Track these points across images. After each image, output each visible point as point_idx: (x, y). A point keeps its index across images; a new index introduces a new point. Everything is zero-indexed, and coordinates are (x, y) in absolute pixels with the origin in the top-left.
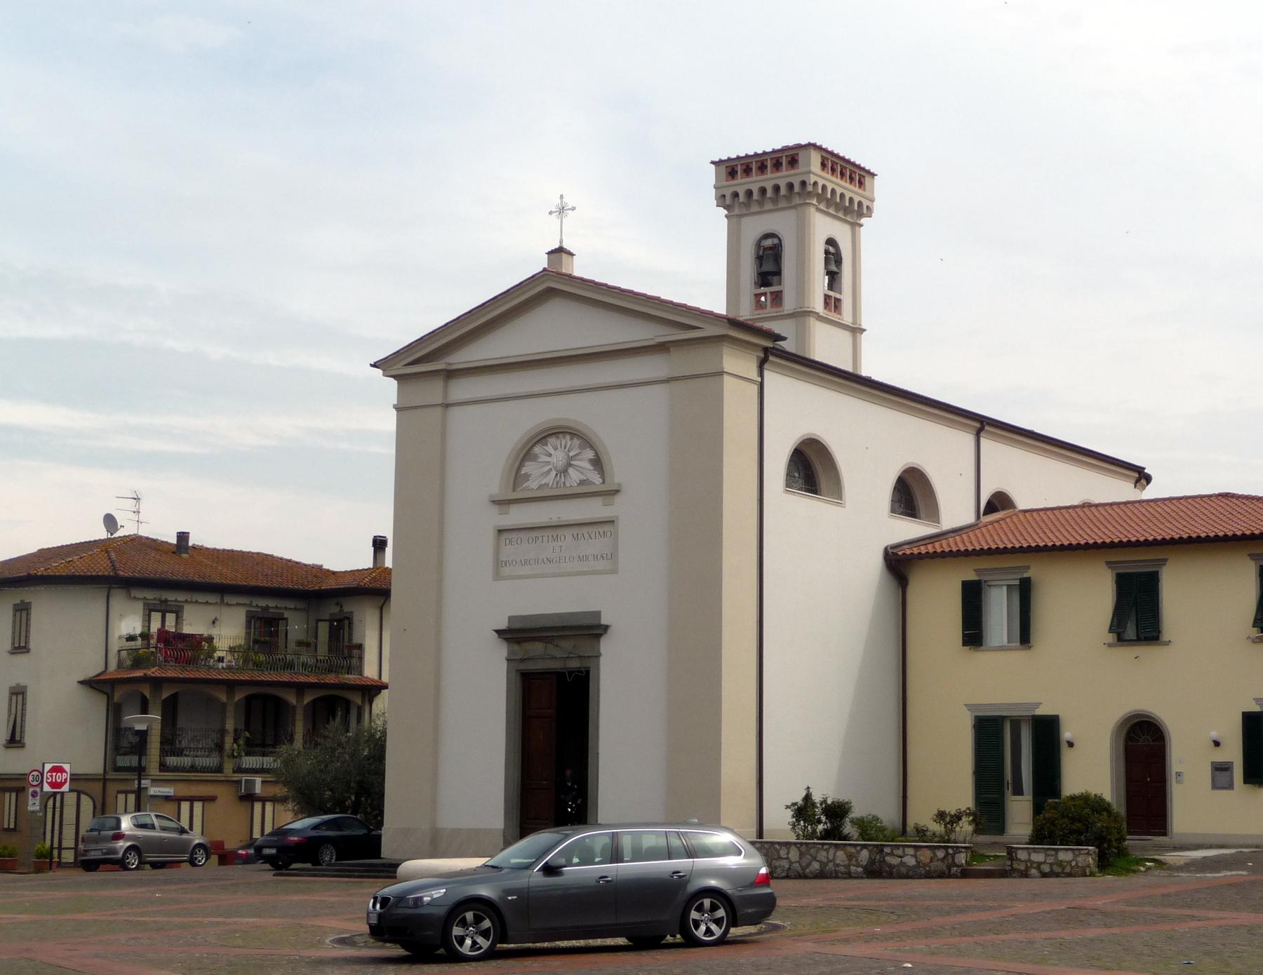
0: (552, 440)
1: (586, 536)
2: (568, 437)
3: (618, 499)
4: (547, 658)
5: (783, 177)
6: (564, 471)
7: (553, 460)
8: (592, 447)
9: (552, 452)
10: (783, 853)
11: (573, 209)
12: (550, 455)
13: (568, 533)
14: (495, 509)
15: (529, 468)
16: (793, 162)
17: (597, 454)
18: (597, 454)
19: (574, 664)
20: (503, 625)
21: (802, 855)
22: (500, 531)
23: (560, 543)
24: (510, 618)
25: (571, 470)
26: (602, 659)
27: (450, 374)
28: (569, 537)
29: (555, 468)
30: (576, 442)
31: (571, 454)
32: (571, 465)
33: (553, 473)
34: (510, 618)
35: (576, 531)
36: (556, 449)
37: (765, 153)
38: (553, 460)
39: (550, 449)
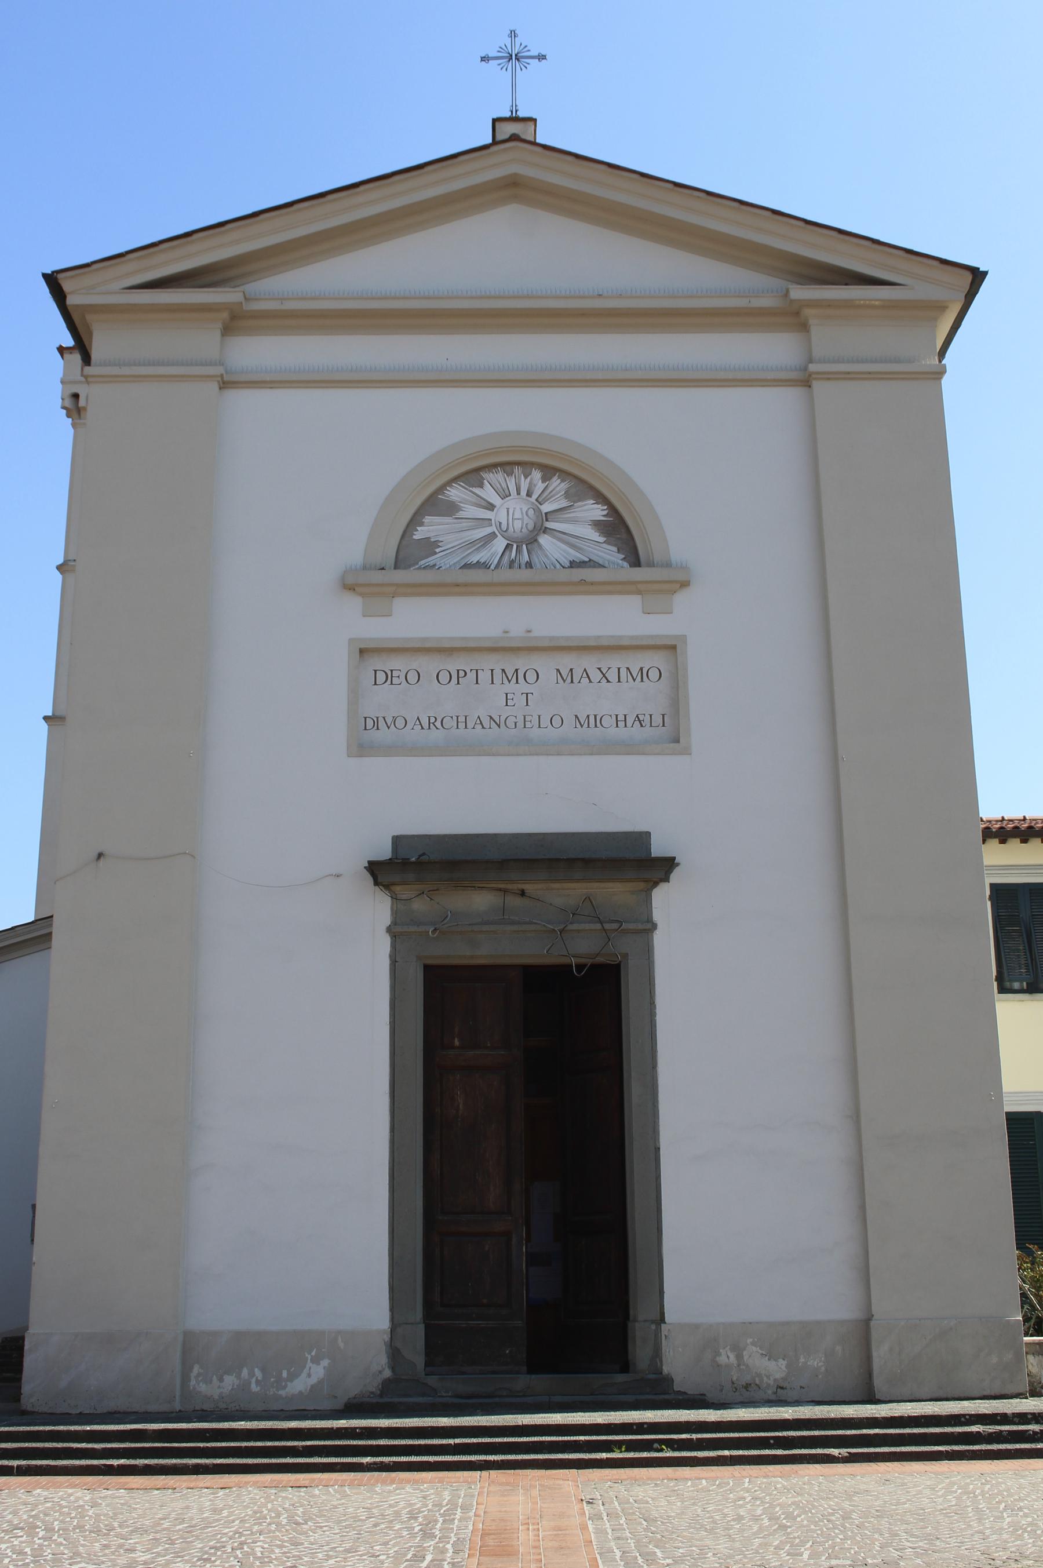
1: (596, 676)
2: (537, 475)
3: (681, 599)
4: (498, 932)
6: (531, 540)
7: (500, 516)
8: (601, 498)
9: (495, 499)
11: (541, 57)
12: (491, 507)
13: (546, 666)
14: (354, 603)
15: (431, 528)
18: (613, 510)
19: (582, 947)
20: (384, 852)
22: (362, 651)
23: (523, 687)
24: (397, 840)
25: (544, 540)
26: (659, 939)
27: (236, 322)
28: (548, 675)
29: (504, 533)
30: (558, 485)
31: (546, 508)
32: (546, 530)
33: (500, 544)
34: (397, 840)
35: (566, 662)
36: (505, 495)
39: (488, 493)
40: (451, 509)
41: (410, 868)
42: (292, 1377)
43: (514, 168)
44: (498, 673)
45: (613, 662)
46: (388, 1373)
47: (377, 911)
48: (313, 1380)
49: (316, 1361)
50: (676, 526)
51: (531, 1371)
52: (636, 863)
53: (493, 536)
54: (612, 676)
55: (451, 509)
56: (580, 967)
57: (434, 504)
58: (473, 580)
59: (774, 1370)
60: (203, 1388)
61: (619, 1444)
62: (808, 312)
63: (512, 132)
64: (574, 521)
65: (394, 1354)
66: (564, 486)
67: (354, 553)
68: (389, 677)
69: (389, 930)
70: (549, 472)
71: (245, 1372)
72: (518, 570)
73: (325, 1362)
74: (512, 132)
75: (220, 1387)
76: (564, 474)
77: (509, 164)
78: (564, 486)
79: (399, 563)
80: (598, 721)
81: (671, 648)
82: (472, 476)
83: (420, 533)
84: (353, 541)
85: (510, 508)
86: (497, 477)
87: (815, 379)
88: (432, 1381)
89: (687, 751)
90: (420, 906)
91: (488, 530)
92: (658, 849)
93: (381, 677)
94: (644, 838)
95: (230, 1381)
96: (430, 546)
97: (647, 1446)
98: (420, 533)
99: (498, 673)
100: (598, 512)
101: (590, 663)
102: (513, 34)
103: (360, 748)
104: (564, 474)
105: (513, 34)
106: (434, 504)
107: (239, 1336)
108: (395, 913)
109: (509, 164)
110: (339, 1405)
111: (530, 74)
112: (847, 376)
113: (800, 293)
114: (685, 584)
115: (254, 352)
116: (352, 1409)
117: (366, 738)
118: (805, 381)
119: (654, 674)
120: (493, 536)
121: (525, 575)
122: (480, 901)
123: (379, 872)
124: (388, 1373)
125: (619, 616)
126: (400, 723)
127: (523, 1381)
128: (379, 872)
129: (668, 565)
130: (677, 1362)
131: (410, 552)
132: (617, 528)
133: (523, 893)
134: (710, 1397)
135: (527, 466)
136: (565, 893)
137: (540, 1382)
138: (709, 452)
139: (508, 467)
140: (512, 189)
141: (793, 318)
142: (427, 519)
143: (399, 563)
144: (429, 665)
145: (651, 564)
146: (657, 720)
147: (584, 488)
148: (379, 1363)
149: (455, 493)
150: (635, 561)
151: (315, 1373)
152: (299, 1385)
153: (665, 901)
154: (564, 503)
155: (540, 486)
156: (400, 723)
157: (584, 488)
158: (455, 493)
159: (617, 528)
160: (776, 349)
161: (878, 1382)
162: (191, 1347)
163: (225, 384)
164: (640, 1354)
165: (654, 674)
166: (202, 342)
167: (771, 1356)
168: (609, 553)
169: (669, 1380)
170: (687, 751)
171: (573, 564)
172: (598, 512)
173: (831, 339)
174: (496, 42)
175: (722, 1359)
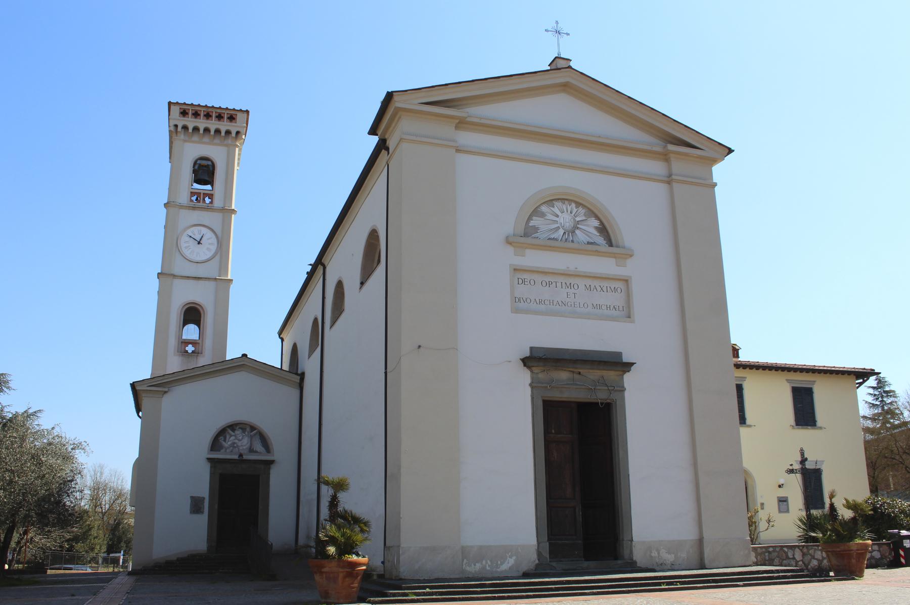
0: (558, 204)
1: (599, 289)
2: (573, 205)
3: (629, 261)
4: (571, 388)
5: (224, 126)
6: (573, 232)
7: (561, 220)
9: (559, 214)
10: (790, 555)
11: (568, 34)
12: (557, 216)
13: (581, 283)
14: (510, 250)
15: (536, 222)
16: (232, 118)
17: (602, 223)
18: (602, 223)
19: (601, 396)
21: (804, 555)
22: (515, 270)
23: (573, 291)
24: (531, 349)
25: (577, 232)
26: (627, 394)
27: (462, 124)
28: (582, 287)
30: (582, 211)
31: (578, 219)
33: (561, 232)
34: (531, 349)
35: (589, 282)
37: (213, 107)
38: (561, 220)
40: (543, 215)
41: (537, 360)
42: (502, 564)
43: (561, 77)
44: (564, 285)
45: (605, 284)
46: (537, 562)
47: (525, 376)
48: (510, 565)
49: (511, 557)
50: (627, 231)
51: (587, 560)
52: (618, 364)
53: (558, 228)
54: (605, 289)
55: (543, 215)
56: (602, 404)
57: (536, 212)
58: (551, 245)
59: (669, 558)
60: (468, 569)
61: (663, 583)
62: (672, 155)
63: (559, 65)
64: (587, 225)
65: (539, 554)
66: (584, 211)
67: (509, 229)
68: (524, 281)
69: (530, 385)
70: (578, 204)
71: (484, 562)
72: (566, 242)
73: (514, 558)
74: (559, 65)
75: (474, 568)
76: (584, 206)
77: (560, 78)
78: (584, 211)
79: (526, 235)
80: (600, 307)
81: (626, 281)
82: (550, 202)
83: (532, 223)
84: (509, 225)
85: (564, 217)
86: (559, 204)
87: (678, 181)
88: (554, 564)
89: (633, 322)
90: (541, 376)
91: (556, 226)
92: (625, 359)
93: (520, 281)
94: (619, 354)
95: (478, 566)
96: (536, 229)
97: (671, 583)
98: (532, 223)
99: (564, 285)
100: (596, 223)
101: (597, 283)
102: (557, 22)
103: (516, 310)
104: (584, 206)
105: (557, 22)
106: (536, 212)
107: (481, 547)
108: (532, 378)
109: (560, 78)
110: (521, 573)
111: (564, 39)
112: (692, 183)
113: (671, 147)
114: (631, 256)
115: (467, 138)
116: (526, 575)
117: (518, 305)
118: (669, 180)
119: (619, 290)
120: (558, 228)
121: (570, 245)
122: (563, 375)
123: (526, 362)
124: (537, 562)
125: (605, 265)
126: (528, 301)
127: (586, 564)
128: (526, 362)
129: (624, 247)
130: (638, 556)
131: (529, 231)
132: (603, 230)
133: (580, 373)
134: (656, 568)
135: (570, 201)
136: (594, 374)
137: (592, 564)
138: (635, 203)
139: (563, 200)
140: (565, 87)
141: (665, 157)
142: (534, 218)
143: (526, 235)
144: (538, 278)
145: (618, 246)
146: (621, 309)
147: (592, 213)
148: (534, 557)
149: (544, 208)
150: (610, 244)
151: (511, 561)
152: (505, 567)
153: (629, 379)
154: (584, 218)
155: (575, 210)
156: (528, 301)
157: (592, 213)
158: (544, 208)
159: (603, 230)
160: (657, 167)
161: (706, 562)
162: (464, 551)
163: (458, 151)
164: (626, 553)
165: (619, 290)
166: (446, 130)
167: (669, 553)
168: (601, 240)
169: (636, 562)
170: (633, 322)
171: (588, 243)
172: (596, 223)
173: (678, 167)
174: (551, 25)
175: (653, 555)
